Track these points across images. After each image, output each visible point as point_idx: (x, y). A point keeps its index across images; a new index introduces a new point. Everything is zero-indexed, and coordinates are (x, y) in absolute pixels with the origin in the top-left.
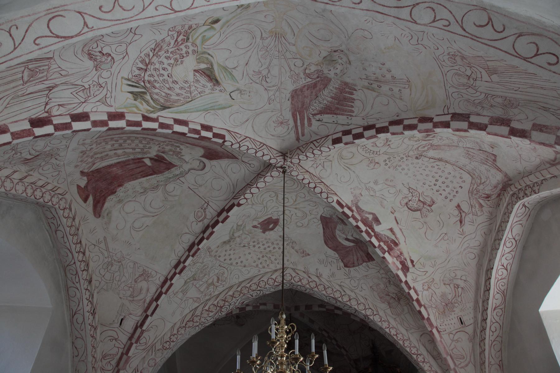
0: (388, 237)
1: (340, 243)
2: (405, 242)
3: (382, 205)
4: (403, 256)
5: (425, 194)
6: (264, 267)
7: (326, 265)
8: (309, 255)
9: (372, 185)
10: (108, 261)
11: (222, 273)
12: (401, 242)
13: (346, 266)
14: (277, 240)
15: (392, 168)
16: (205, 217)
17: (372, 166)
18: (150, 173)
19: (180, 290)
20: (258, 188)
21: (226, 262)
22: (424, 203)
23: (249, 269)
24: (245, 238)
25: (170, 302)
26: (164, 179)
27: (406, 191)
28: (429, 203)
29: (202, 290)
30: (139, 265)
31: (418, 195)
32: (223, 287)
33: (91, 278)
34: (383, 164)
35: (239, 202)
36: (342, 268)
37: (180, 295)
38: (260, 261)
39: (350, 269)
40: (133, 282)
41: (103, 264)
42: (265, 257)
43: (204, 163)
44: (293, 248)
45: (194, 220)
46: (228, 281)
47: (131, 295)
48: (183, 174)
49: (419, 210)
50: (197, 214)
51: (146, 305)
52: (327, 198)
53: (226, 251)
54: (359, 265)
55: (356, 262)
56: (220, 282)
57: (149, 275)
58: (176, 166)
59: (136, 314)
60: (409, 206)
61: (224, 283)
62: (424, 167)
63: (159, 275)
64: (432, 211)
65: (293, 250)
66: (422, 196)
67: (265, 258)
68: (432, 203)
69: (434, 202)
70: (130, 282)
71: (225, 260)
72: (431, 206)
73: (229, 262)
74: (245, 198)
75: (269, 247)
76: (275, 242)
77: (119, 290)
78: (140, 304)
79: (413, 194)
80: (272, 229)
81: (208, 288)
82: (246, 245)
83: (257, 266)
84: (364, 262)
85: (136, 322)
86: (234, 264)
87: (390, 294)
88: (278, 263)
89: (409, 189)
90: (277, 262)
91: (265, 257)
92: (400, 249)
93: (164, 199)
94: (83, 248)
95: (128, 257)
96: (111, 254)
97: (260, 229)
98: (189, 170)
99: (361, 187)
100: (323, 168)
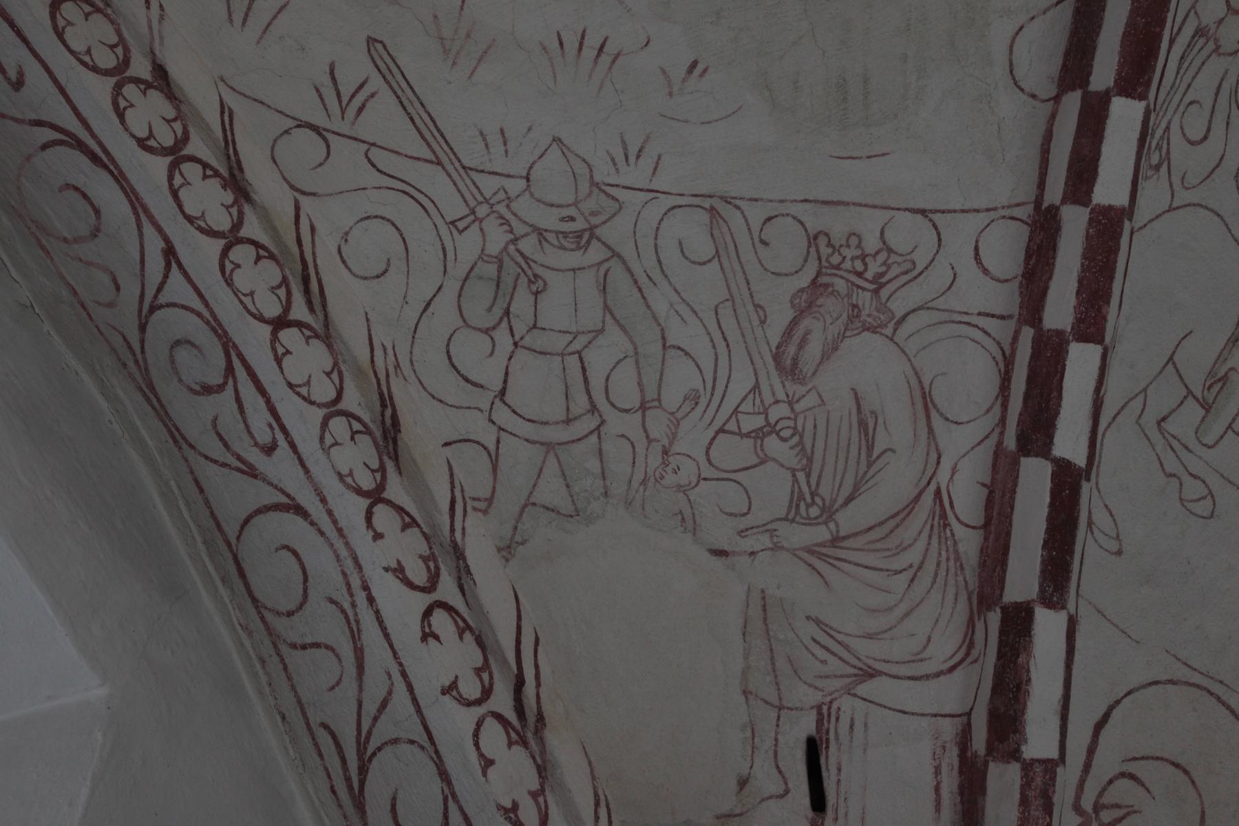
10: (483, 256)
25: (1193, 489)
30: (756, 215)
33: (386, 401)
40: (773, 384)
41: (452, 287)
47: (796, 500)
51: (970, 543)
57: (874, 268)
59: (917, 659)
63: (964, 229)
70: (741, 384)
77: (682, 489)
78: (913, 556)
85: (949, 729)
94: (206, 128)
95: (636, 175)
96: (489, 185)
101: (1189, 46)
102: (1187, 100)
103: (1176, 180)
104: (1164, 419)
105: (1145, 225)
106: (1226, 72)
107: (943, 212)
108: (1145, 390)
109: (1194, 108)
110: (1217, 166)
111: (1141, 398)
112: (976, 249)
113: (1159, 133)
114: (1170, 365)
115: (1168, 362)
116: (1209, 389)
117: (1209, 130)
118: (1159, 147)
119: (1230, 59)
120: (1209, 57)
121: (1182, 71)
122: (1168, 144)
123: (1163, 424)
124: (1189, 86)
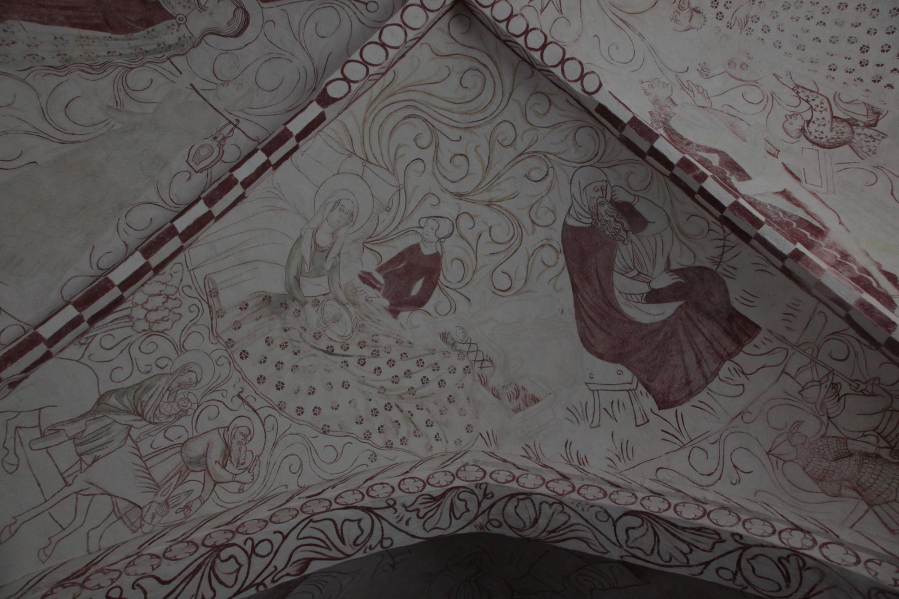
0: (784, 213)
1: (631, 322)
2: (840, 223)
3: (736, 134)
4: (854, 262)
5: (845, 98)
6: (389, 445)
7: (596, 423)
8: (535, 400)
9: (694, 76)
11: (245, 431)
12: (827, 224)
13: (663, 403)
14: (433, 352)
15: (736, 28)
16: (219, 159)
17: (684, 15)
18: (96, 21)
19: (72, 430)
20: (383, 45)
21: (261, 388)
22: (852, 123)
23: (339, 442)
24: (336, 320)
25: (12, 459)
26: (129, 51)
27: (789, 97)
28: (865, 119)
29: (159, 473)
31: (826, 105)
32: (241, 491)
34: (710, 13)
35: (325, 90)
36: (651, 417)
37: (66, 454)
38: (378, 422)
39: (680, 409)
42: (394, 407)
43: (246, 12)
44: (485, 384)
45: (185, 167)
46: (263, 473)
48: (184, 47)
49: (845, 143)
50: (198, 151)
52: (582, 77)
53: (269, 342)
54: (707, 381)
55: (696, 377)
56: (229, 466)
58: (171, 17)
60: (811, 137)
61: (245, 477)
62: (819, 17)
64: (884, 136)
65: (483, 389)
66: (837, 105)
67: (395, 414)
68: (872, 117)
69: (879, 114)
71: (261, 379)
72: (875, 125)
73: (276, 396)
74: (345, 79)
75: (408, 374)
76: (428, 360)
79: (813, 104)
80: (419, 303)
81: (182, 475)
82: (337, 350)
83: (368, 436)
84: (722, 358)
86: (291, 409)
87: (853, 446)
88: (437, 438)
89: (796, 89)
90: (432, 432)
91: (395, 408)
92: (835, 244)
93: (112, 103)
97: (385, 295)
98: (203, 36)
99: (667, 82)
100: (557, 14)
101: (122, 317)
102: (110, 332)
103: (87, 354)
104: (20, 428)
105: (63, 359)
106: (132, 336)
107: (6, 313)
108: (20, 412)
109: (110, 337)
110: (108, 361)
111: (15, 414)
112: (4, 329)
113: (91, 334)
114: (38, 411)
115: (37, 409)
116: (48, 430)
117: (112, 348)
118: (87, 339)
119: (135, 333)
120: (128, 326)
121: (114, 323)
122: (92, 340)
123: (18, 429)
124: (114, 329)
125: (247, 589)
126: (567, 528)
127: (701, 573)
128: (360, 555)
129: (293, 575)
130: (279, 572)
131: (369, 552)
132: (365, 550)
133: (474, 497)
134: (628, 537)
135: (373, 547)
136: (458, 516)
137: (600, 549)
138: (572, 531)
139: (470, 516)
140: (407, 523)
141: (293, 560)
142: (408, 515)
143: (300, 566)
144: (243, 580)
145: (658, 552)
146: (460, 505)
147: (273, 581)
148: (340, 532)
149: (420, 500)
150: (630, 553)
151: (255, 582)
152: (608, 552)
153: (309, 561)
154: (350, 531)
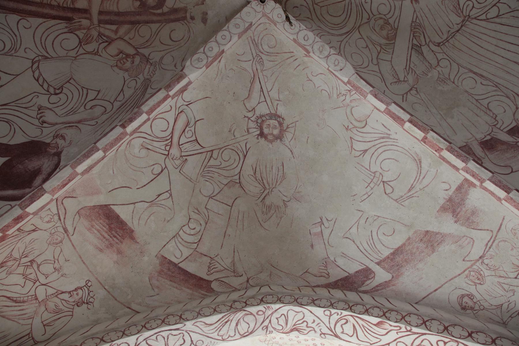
125: (418, 333)
126: (219, 328)
127: (137, 339)
128: (345, 313)
129: (387, 323)
130: (396, 330)
131: (339, 311)
132: (341, 314)
133: (273, 326)
134: (183, 339)
135: (336, 314)
136: (283, 316)
137: (197, 324)
138: (216, 328)
139: (276, 315)
140: (314, 321)
141: (386, 331)
142: (314, 325)
143: (382, 326)
144: (418, 339)
145: (164, 338)
146: (282, 321)
147: (401, 328)
148: (355, 332)
149: (306, 332)
150: (180, 330)
151: (411, 333)
152: (193, 325)
153: (376, 325)
154: (348, 328)
